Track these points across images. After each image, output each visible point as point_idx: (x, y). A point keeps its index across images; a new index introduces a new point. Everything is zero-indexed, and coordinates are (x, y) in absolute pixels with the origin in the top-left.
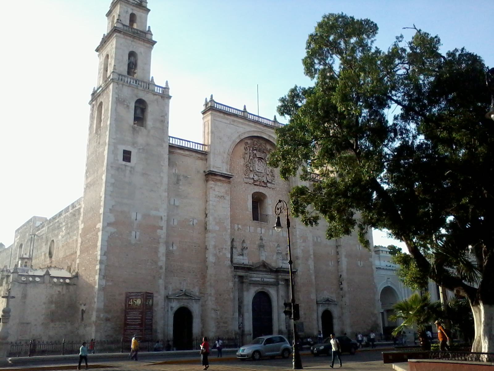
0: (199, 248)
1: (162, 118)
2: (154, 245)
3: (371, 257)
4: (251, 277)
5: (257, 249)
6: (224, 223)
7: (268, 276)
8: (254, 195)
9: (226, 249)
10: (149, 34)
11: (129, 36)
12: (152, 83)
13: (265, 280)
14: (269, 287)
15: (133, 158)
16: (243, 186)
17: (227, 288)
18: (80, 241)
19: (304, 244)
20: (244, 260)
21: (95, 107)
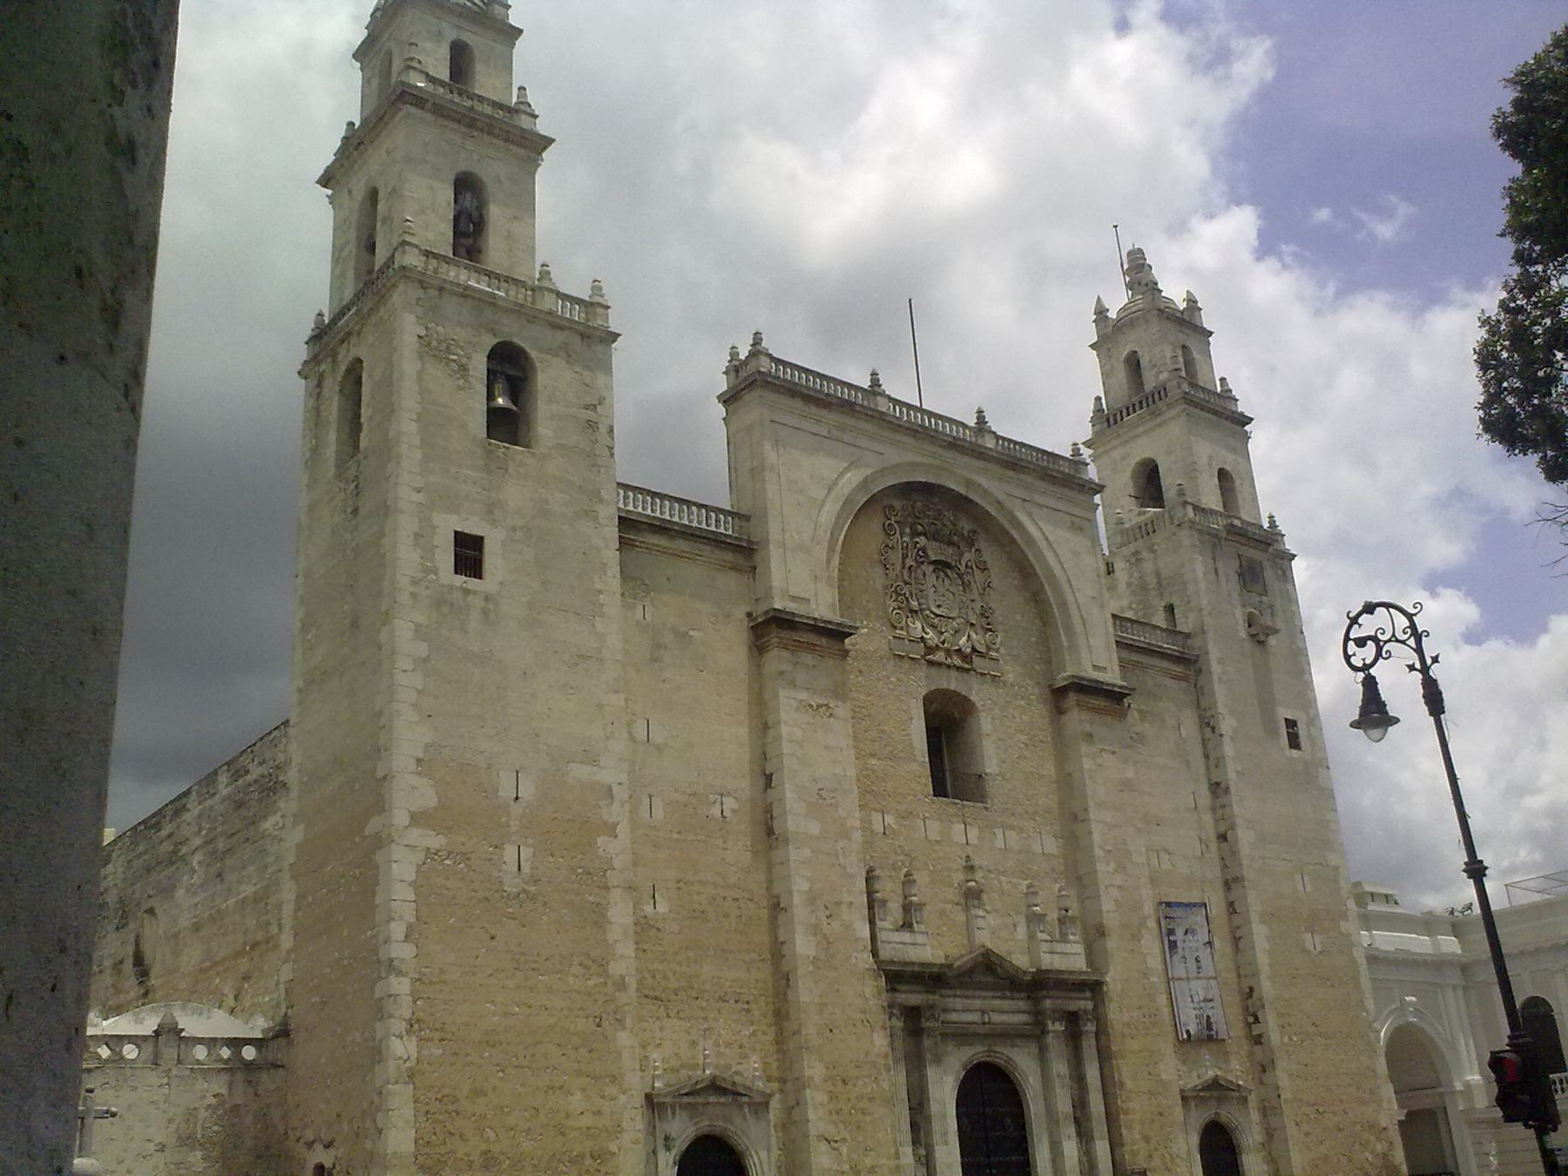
0: (751, 905)
1: (590, 414)
2: (591, 899)
3: (1344, 916)
4: (945, 1011)
5: (957, 904)
6: (835, 806)
7: (1006, 1004)
8: (928, 700)
9: (852, 903)
10: (525, 113)
11: (453, 119)
12: (545, 284)
13: (997, 1018)
14: (1012, 1046)
15: (492, 558)
17: (867, 1054)
18: (288, 892)
19: (1118, 880)
21: (328, 383)
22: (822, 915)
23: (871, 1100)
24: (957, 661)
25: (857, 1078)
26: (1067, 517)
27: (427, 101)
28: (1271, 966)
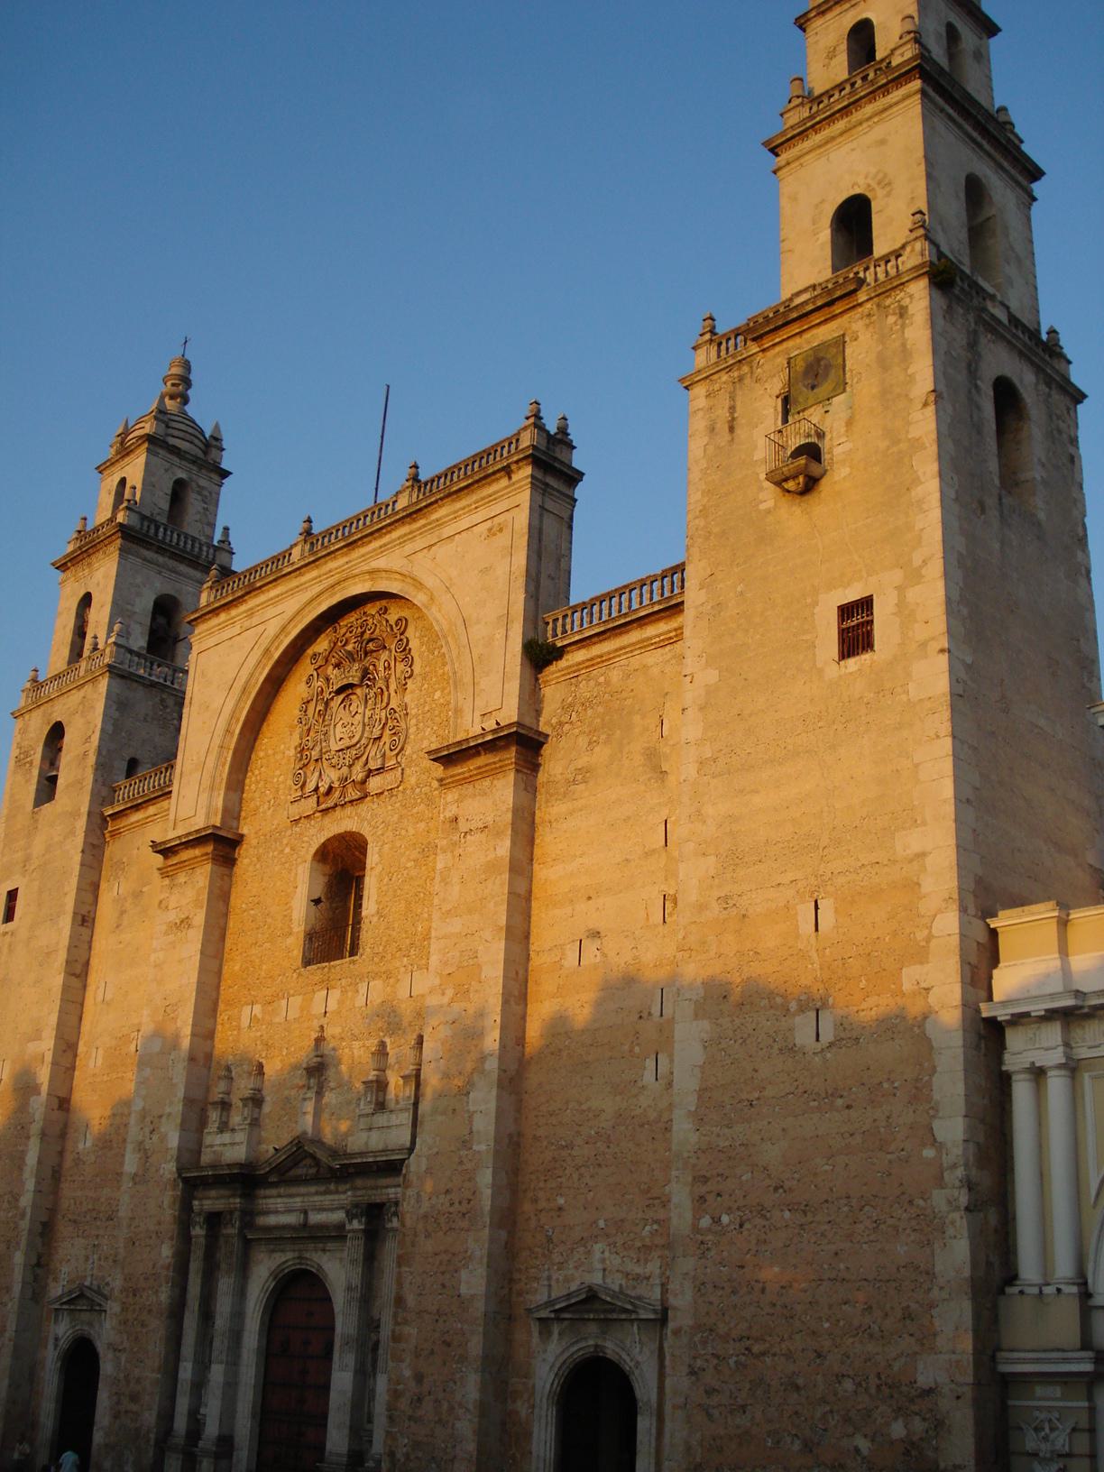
7: (327, 1200)
9: (170, 1114)
13: (315, 1218)
14: (324, 1250)
16: (285, 841)
20: (229, 1147)
22: (147, 1134)
23: (150, 1311)
25: (144, 1289)
26: (489, 524)
27: (66, 563)
28: (702, 1092)
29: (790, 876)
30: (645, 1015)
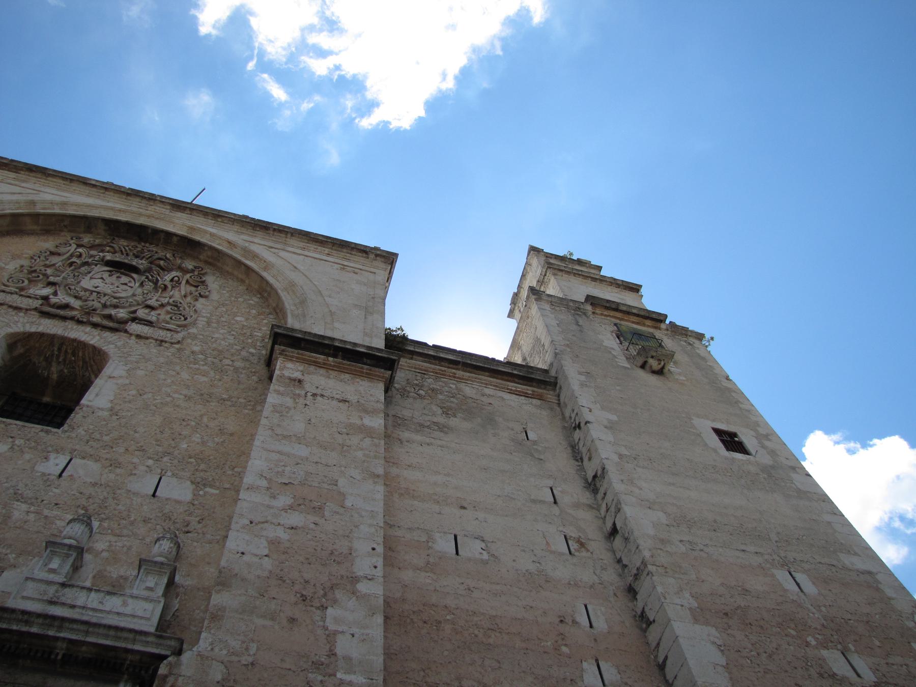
19: (295, 519)
24: (96, 319)
29: (751, 549)
30: (568, 620)
